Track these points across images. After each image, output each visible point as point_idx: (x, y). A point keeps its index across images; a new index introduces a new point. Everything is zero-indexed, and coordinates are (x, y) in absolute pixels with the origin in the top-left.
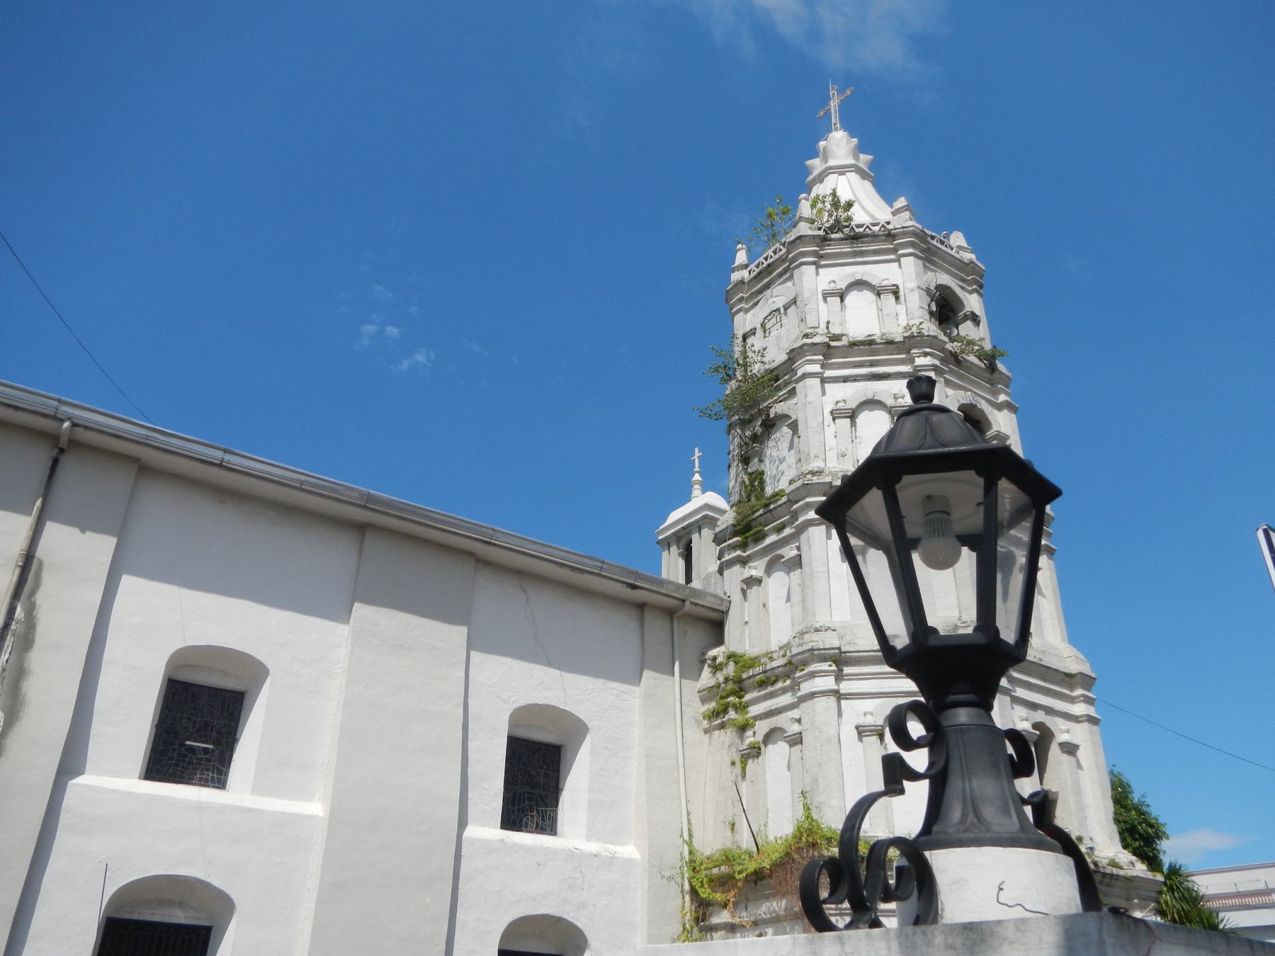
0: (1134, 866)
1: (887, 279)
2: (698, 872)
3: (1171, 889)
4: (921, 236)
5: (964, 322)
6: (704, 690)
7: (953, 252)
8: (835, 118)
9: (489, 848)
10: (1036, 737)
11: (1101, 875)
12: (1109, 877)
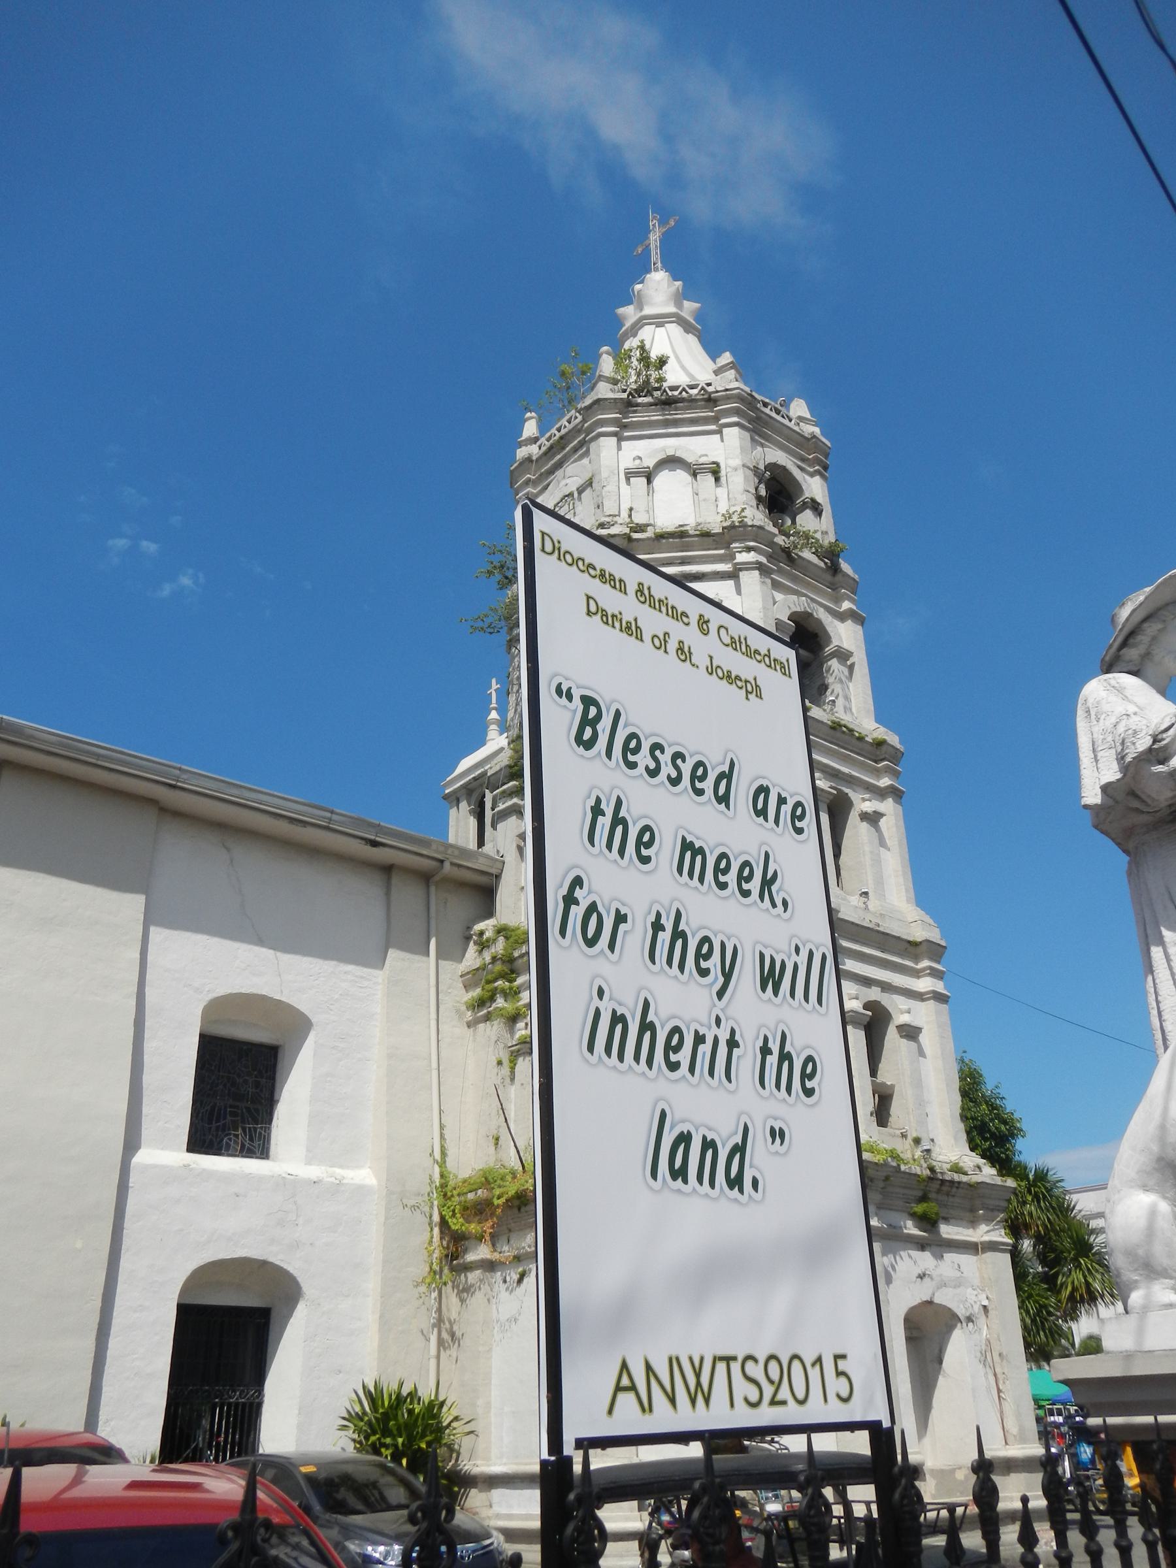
0: (981, 1171)
1: (706, 455)
2: (449, 1199)
3: (1036, 1197)
4: (749, 401)
5: (802, 511)
6: (468, 973)
7: (791, 425)
8: (655, 256)
9: (167, 1175)
10: (868, 1019)
11: (939, 1182)
12: (948, 1184)
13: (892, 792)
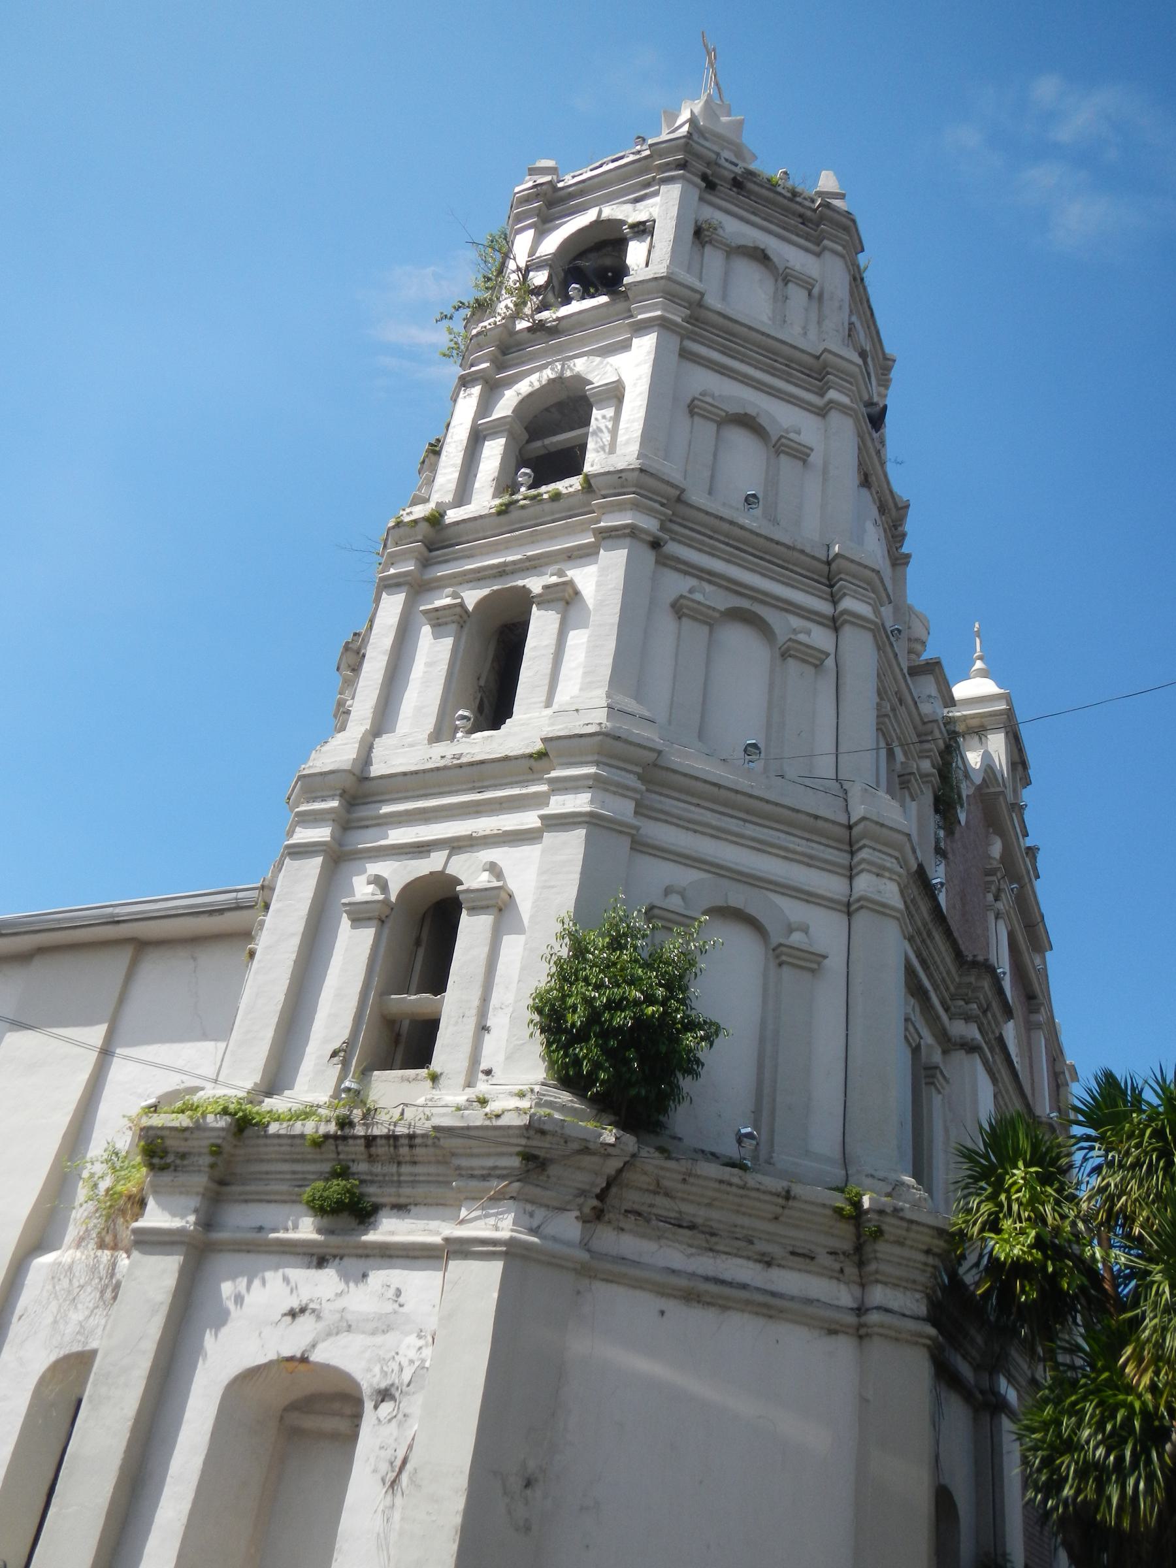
11: (362, 1141)
12: (383, 1142)
13: (604, 538)
